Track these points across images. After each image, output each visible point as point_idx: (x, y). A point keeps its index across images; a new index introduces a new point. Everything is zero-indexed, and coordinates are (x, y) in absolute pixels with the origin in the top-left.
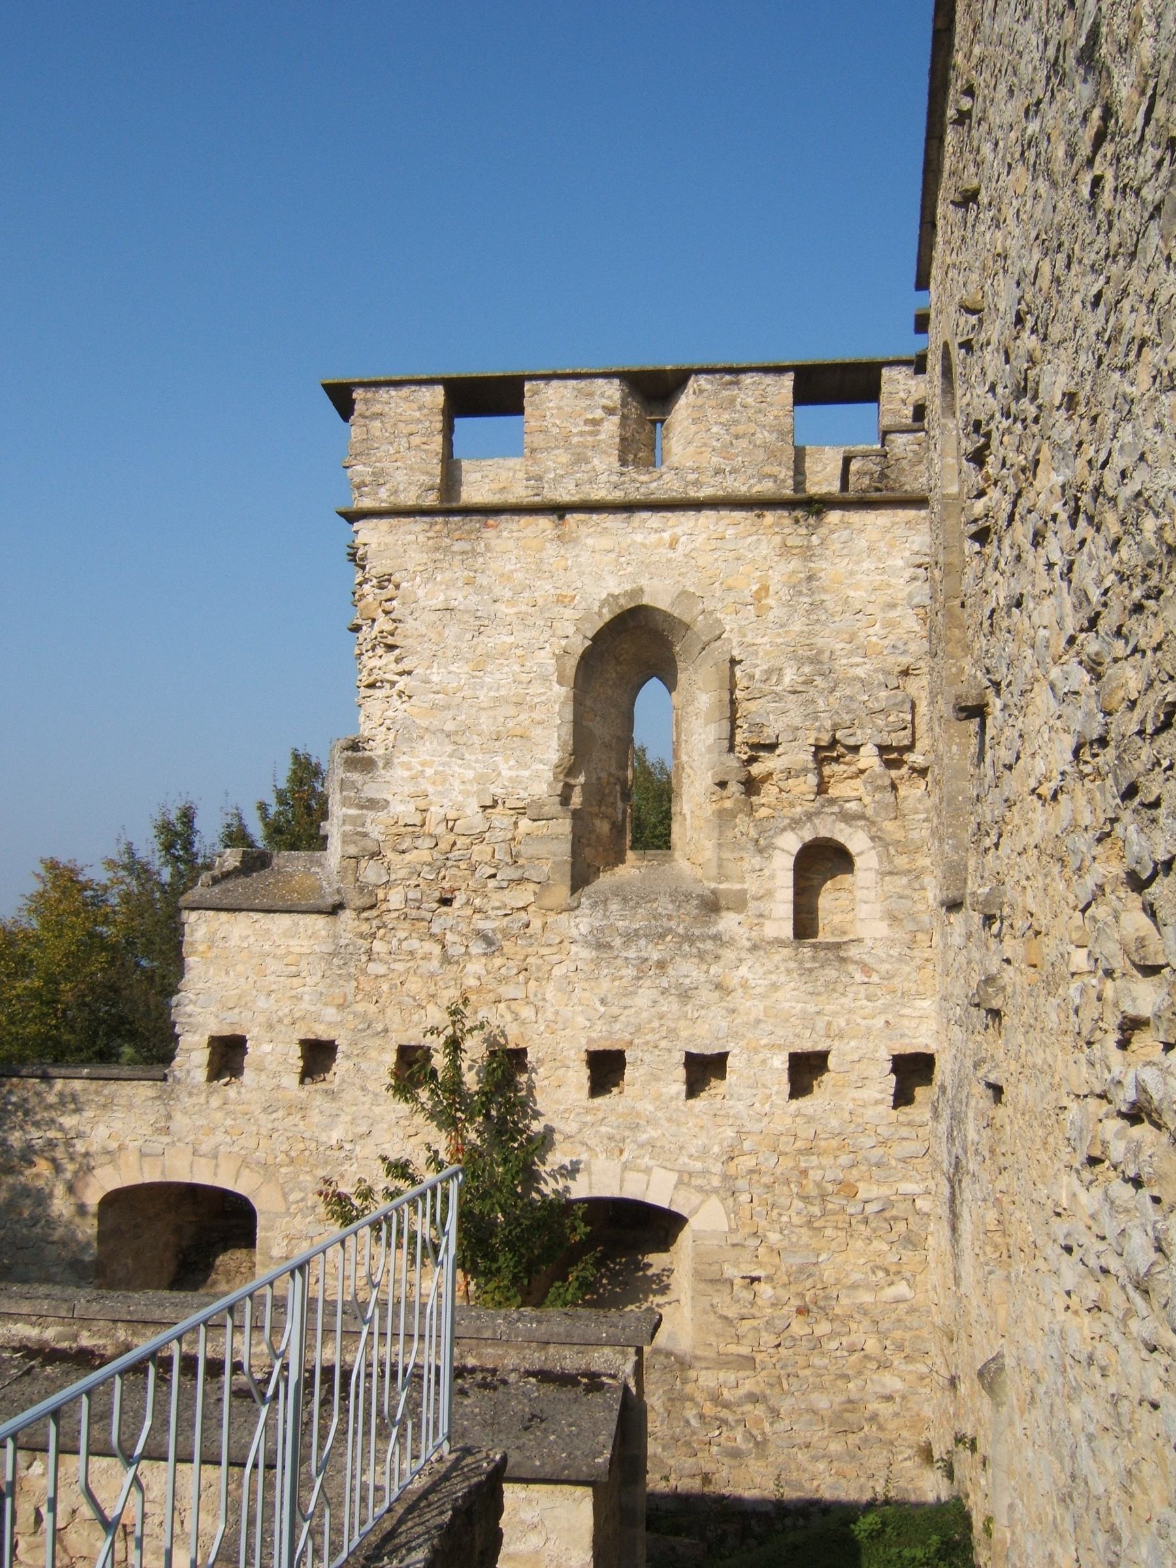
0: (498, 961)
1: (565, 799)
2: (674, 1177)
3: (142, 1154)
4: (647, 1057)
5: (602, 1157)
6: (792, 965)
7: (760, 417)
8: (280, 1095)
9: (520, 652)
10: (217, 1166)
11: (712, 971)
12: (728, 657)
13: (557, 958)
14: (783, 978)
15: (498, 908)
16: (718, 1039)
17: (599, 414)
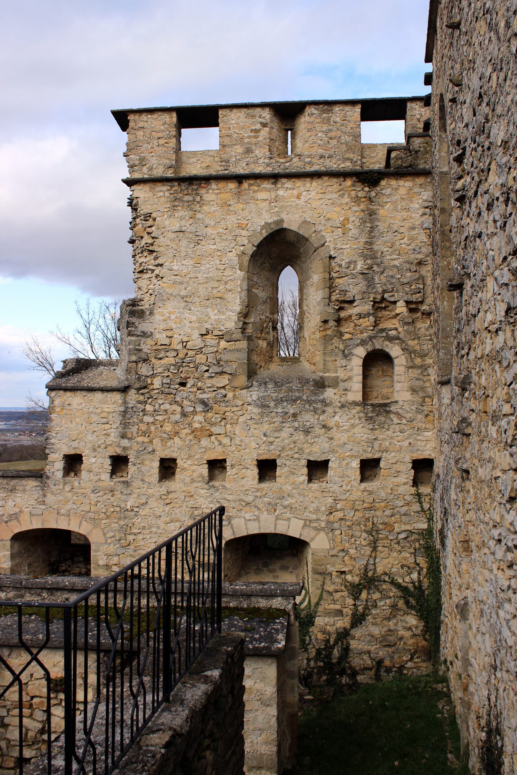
0: (210, 415)
1: (243, 330)
2: (303, 522)
3: (31, 515)
4: (288, 463)
5: (265, 513)
6: (362, 415)
7: (343, 128)
8: (100, 484)
9: (219, 253)
10: (69, 520)
11: (321, 419)
12: (328, 255)
13: (240, 413)
14: (357, 421)
15: (210, 387)
16: (324, 453)
17: (258, 126)
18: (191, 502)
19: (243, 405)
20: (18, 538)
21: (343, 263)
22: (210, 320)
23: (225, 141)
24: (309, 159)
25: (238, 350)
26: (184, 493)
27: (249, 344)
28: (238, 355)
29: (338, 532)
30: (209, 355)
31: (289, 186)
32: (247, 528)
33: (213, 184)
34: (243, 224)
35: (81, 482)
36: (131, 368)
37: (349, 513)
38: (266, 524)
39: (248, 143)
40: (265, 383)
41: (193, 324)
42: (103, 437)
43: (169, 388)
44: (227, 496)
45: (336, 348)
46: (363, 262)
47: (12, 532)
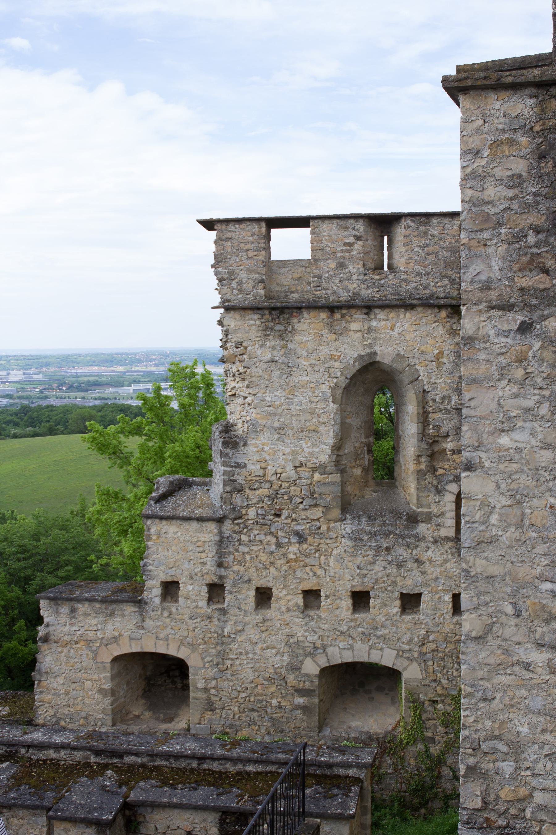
0: (305, 546)
1: (337, 463)
2: (396, 652)
3: (131, 639)
4: (381, 595)
5: (360, 643)
6: (454, 550)
7: (442, 243)
8: (198, 611)
9: (312, 385)
10: (168, 644)
11: (414, 553)
12: (422, 390)
13: (335, 545)
14: (450, 557)
15: (304, 519)
16: (417, 586)
17: (352, 240)
18: (287, 630)
19: (337, 537)
20: (117, 659)
21: (437, 398)
22: (303, 453)
23: (317, 255)
24: (405, 276)
25: (332, 484)
26: (280, 622)
27: (342, 477)
28: (332, 488)
29: (430, 663)
30: (303, 488)
31: (382, 317)
32: (341, 657)
33: (304, 313)
34: (335, 356)
35: (179, 608)
36: (225, 498)
37: (441, 645)
38: (360, 653)
39: (342, 257)
40: (359, 517)
41: (287, 457)
42: (200, 565)
43: (264, 519)
44: (321, 625)
45: (429, 483)
46: (457, 397)
47: (112, 654)
